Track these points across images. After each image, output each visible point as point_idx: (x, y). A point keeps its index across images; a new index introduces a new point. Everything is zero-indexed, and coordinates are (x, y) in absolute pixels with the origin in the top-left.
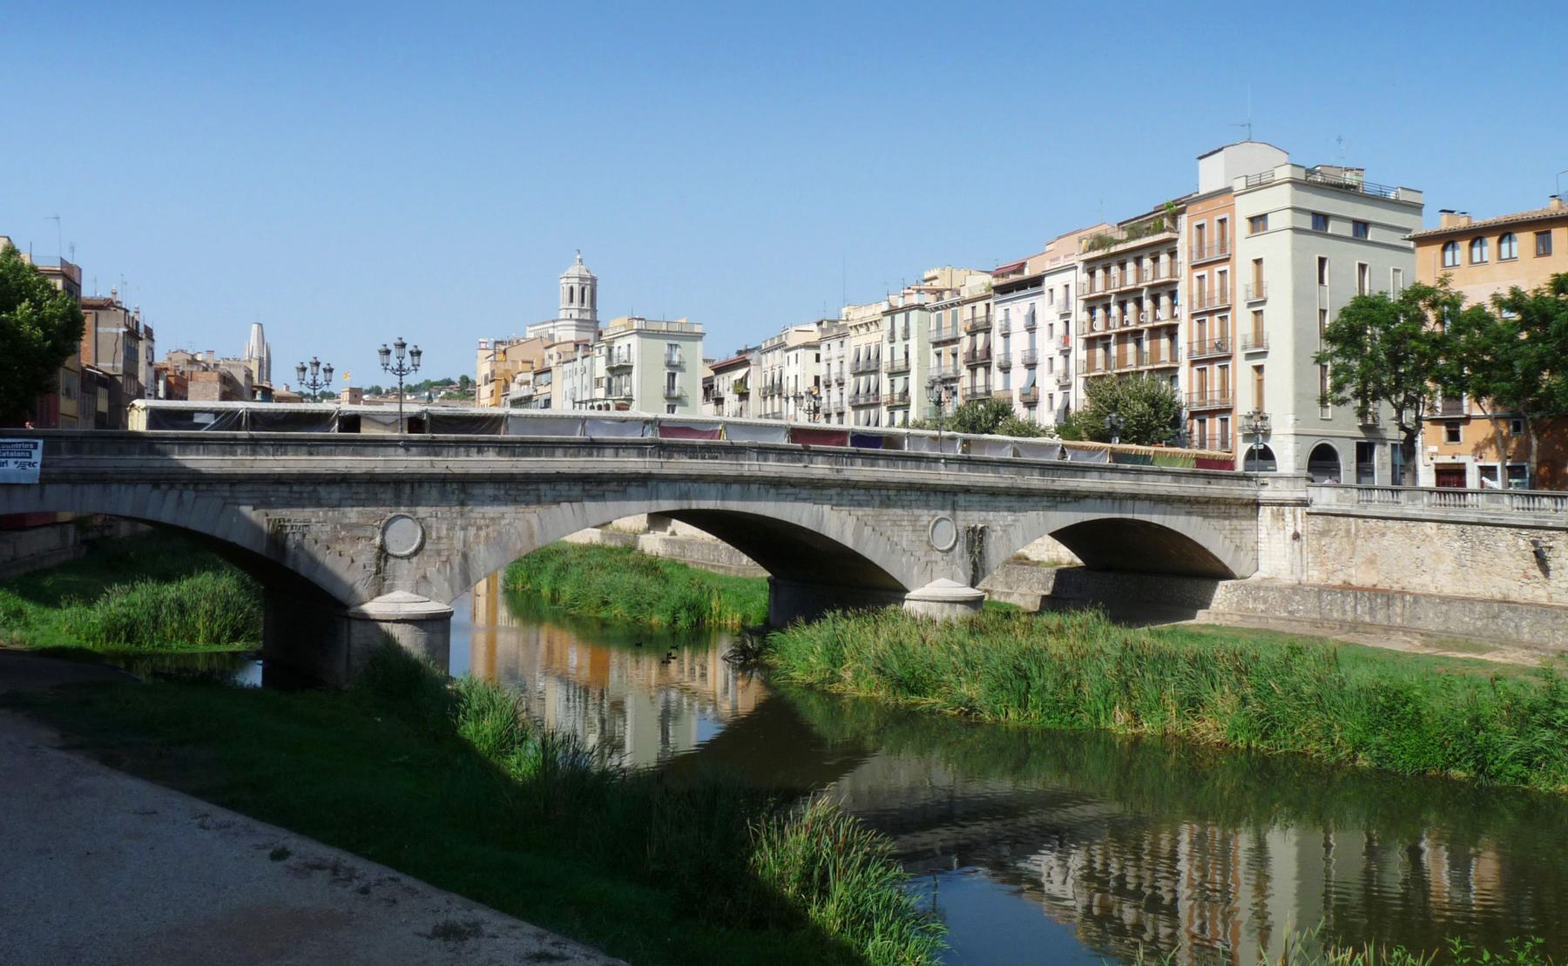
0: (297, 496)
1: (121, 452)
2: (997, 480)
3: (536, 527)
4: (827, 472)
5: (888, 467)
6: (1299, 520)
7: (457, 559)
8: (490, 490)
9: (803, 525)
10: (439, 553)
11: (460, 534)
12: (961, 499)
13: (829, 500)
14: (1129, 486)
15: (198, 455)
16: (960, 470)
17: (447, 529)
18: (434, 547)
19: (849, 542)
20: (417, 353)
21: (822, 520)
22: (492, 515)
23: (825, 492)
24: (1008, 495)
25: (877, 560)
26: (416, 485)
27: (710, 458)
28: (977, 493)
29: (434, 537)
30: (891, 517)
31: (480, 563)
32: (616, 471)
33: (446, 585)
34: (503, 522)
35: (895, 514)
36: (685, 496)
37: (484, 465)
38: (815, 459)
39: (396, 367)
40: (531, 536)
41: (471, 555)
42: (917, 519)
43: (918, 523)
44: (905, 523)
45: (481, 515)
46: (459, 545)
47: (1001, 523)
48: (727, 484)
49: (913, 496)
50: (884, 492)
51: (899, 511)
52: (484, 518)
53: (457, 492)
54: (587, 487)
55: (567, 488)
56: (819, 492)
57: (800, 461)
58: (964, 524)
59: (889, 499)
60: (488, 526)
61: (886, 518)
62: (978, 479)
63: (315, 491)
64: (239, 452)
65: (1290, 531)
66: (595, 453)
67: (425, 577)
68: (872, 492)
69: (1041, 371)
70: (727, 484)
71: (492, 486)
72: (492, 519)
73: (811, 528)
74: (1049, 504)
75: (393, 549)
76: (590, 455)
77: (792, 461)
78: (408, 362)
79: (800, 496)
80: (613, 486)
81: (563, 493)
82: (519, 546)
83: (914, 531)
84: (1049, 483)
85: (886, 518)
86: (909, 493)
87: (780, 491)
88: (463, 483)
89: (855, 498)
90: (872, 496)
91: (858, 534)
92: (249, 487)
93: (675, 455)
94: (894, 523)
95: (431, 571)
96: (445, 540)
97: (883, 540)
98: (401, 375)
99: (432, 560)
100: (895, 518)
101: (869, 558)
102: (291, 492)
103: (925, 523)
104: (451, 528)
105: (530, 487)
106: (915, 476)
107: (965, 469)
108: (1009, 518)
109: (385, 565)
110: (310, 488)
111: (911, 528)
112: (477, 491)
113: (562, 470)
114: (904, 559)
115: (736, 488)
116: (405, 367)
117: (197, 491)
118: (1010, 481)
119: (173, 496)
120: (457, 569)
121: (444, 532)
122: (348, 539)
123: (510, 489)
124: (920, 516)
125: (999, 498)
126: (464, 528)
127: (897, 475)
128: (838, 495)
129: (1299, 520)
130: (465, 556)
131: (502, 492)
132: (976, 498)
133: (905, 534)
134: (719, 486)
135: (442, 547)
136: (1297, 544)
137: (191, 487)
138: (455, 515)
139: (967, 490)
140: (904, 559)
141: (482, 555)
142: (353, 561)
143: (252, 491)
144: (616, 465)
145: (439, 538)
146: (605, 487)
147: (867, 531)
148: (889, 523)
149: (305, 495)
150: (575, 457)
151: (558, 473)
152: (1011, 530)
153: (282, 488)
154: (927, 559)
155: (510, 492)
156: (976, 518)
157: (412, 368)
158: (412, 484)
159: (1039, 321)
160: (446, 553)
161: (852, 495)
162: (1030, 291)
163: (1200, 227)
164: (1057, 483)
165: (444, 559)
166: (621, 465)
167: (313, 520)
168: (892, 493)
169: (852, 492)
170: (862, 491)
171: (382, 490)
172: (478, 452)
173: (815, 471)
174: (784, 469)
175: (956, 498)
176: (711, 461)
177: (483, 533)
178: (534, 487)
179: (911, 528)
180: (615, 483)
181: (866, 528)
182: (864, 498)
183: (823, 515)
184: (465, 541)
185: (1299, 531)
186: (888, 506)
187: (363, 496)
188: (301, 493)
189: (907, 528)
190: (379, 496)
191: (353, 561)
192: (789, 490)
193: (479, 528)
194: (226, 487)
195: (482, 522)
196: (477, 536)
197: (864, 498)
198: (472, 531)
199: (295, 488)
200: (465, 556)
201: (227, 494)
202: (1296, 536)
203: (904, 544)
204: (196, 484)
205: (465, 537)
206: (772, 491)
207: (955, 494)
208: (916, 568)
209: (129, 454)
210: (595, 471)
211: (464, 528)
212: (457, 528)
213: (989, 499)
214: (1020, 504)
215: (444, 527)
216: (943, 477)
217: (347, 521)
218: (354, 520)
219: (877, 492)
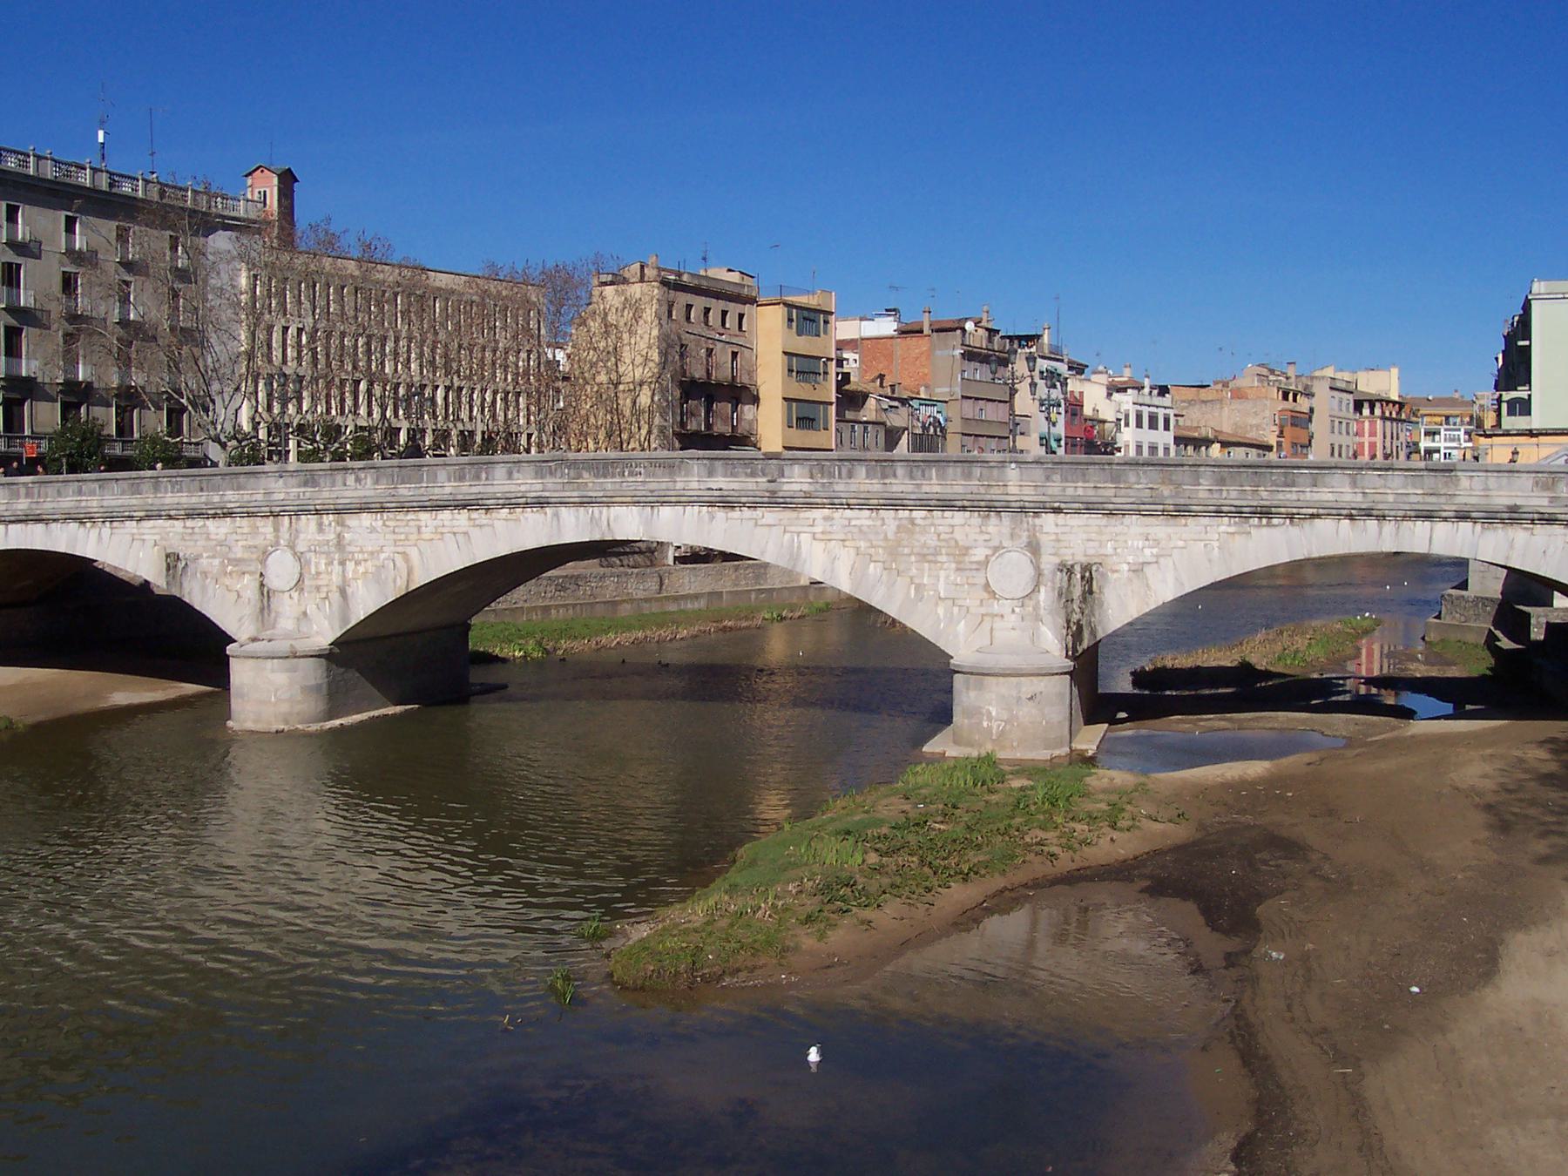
0: (190, 531)
7: (335, 596)
10: (318, 588)
11: (337, 568)
14: (1420, 499)
17: (326, 564)
18: (314, 583)
22: (370, 549)
24: (1139, 513)
27: (631, 474)
29: (313, 571)
30: (915, 551)
31: (359, 601)
33: (326, 623)
34: (383, 556)
40: (410, 573)
41: (349, 591)
43: (967, 559)
44: (943, 558)
45: (358, 549)
47: (1130, 559)
52: (361, 552)
53: (333, 524)
56: (793, 514)
58: (1057, 560)
59: (913, 524)
60: (366, 560)
61: (906, 551)
67: (305, 614)
72: (372, 553)
74: (1231, 529)
75: (273, 582)
79: (764, 521)
81: (446, 523)
83: (958, 569)
85: (906, 551)
86: (947, 514)
89: (853, 523)
90: (883, 519)
92: (151, 523)
94: (923, 557)
97: (901, 582)
99: (313, 595)
100: (925, 551)
102: (185, 527)
103: (982, 558)
104: (330, 563)
108: (1147, 552)
111: (953, 566)
114: (941, 611)
117: (112, 528)
119: (94, 533)
120: (335, 607)
122: (234, 575)
124: (968, 548)
126: (342, 563)
128: (826, 519)
130: (343, 592)
131: (380, 523)
133: (942, 573)
135: (320, 583)
137: (108, 524)
138: (333, 549)
141: (360, 593)
142: (239, 596)
143: (154, 527)
145: (318, 573)
148: (913, 558)
149: (196, 530)
152: (1148, 570)
154: (983, 610)
155: (387, 523)
160: (325, 589)
161: (850, 520)
165: (324, 595)
171: (262, 524)
175: (1037, 521)
176: (631, 479)
177: (361, 569)
179: (953, 566)
181: (872, 565)
182: (870, 522)
183: (799, 547)
184: (344, 576)
187: (246, 530)
188: (193, 528)
189: (946, 566)
190: (260, 530)
191: (239, 596)
193: (358, 563)
195: (361, 556)
196: (355, 571)
197: (870, 522)
199: (189, 523)
200: (343, 592)
201: (135, 531)
211: (342, 563)
212: (336, 562)
213: (1104, 521)
214: (1170, 530)
215: (323, 562)
217: (232, 556)
218: (239, 555)
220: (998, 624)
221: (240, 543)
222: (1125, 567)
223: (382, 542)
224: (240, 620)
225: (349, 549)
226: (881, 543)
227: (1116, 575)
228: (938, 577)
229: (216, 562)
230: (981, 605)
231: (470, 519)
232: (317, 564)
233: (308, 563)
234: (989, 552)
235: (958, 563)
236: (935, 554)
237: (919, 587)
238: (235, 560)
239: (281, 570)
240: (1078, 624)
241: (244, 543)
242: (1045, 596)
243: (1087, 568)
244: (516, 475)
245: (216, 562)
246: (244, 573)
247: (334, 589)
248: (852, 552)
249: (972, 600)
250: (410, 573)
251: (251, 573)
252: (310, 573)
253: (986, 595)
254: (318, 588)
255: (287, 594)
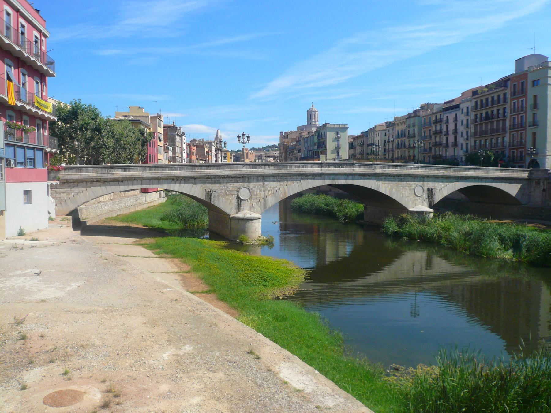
1: (163, 170)
2: (439, 173)
3: (286, 190)
4: (381, 171)
5: (401, 169)
6: (545, 185)
7: (262, 201)
8: (272, 179)
9: (373, 188)
10: (257, 199)
12: (426, 179)
13: (381, 180)
15: (185, 170)
16: (426, 170)
19: (388, 194)
20: (248, 137)
21: (379, 187)
23: (380, 178)
24: (442, 178)
25: (397, 200)
26: (249, 178)
27: (342, 167)
28: (431, 177)
32: (311, 172)
34: (276, 189)
35: (403, 185)
36: (334, 179)
37: (271, 171)
38: (376, 167)
39: (243, 141)
40: (285, 193)
41: (267, 199)
42: (411, 186)
43: (411, 188)
44: (407, 187)
46: (263, 196)
48: (347, 176)
49: (410, 178)
50: (400, 177)
51: (404, 183)
52: (270, 188)
54: (302, 177)
55: (296, 178)
57: (372, 168)
60: (271, 190)
62: (431, 173)
63: (219, 180)
64: (197, 169)
65: (542, 188)
66: (305, 167)
68: (396, 177)
69: (459, 136)
70: (347, 176)
71: (273, 177)
72: (273, 188)
73: (375, 189)
76: (303, 167)
77: (369, 168)
78: (246, 140)
80: (311, 177)
82: (281, 196)
83: (410, 190)
84: (456, 174)
85: (400, 186)
86: (408, 178)
87: (365, 178)
88: (264, 177)
91: (391, 190)
92: (199, 180)
93: (331, 167)
94: (403, 188)
95: (255, 204)
96: (258, 195)
98: (244, 144)
99: (255, 201)
100: (404, 186)
101: (395, 199)
102: (212, 181)
103: (414, 187)
105: (284, 178)
106: (410, 172)
107: (427, 169)
108: (443, 185)
109: (241, 203)
110: (218, 179)
112: (268, 179)
113: (294, 172)
115: (350, 177)
116: (245, 141)
118: (443, 173)
120: (262, 204)
121: (258, 192)
123: (278, 179)
124: (411, 185)
125: (439, 179)
126: (264, 191)
127: (404, 172)
128: (385, 178)
129: (545, 185)
131: (276, 179)
132: (431, 179)
133: (407, 191)
134: (345, 176)
135: (258, 197)
136: (544, 193)
138: (261, 187)
139: (428, 176)
140: (406, 199)
142: (231, 202)
144: (312, 170)
145: (257, 194)
146: (308, 177)
147: (394, 190)
148: (401, 187)
149: (216, 182)
150: (298, 168)
151: (293, 173)
152: (443, 189)
153: (209, 180)
156: (431, 185)
157: (247, 142)
158: (248, 177)
159: (458, 119)
160: (259, 199)
162: (455, 109)
163: (515, 85)
164: (459, 174)
166: (313, 170)
167: (219, 189)
168: (402, 178)
169: (389, 177)
170: (392, 177)
171: (239, 180)
172: (268, 167)
173: (376, 171)
174: (366, 171)
175: (424, 179)
177: (270, 193)
178: (286, 178)
180: (311, 176)
185: (545, 188)
186: (401, 181)
188: (215, 181)
191: (231, 202)
192: (368, 177)
193: (269, 191)
194: (193, 180)
196: (268, 193)
198: (267, 192)
199: (213, 180)
202: (544, 190)
203: (407, 194)
204: (184, 179)
205: (265, 193)
206: (362, 177)
207: (424, 178)
208: (410, 202)
209: (166, 171)
210: (305, 172)
211: (264, 191)
212: (262, 191)
213: (435, 179)
216: (420, 172)
217: (229, 189)
219: (397, 177)
220: (417, 202)
221: (231, 186)
222: (439, 189)
223: (276, 185)
224: (231, 208)
225: (268, 187)
226: (395, 184)
227: (437, 191)
228: (406, 192)
229: (223, 192)
230: (414, 197)
231: (301, 178)
232: (256, 191)
233: (254, 191)
234: (415, 186)
235: (410, 188)
236: (405, 187)
237: (403, 194)
238: (230, 190)
239: (244, 194)
240: (431, 201)
241: (233, 185)
242: (425, 195)
243: (432, 189)
244: (313, 167)
245: (223, 192)
246: (232, 195)
247: (262, 199)
248: (390, 186)
249: (412, 196)
250: (285, 193)
251: (235, 194)
252: (254, 194)
253: (415, 195)
254: (257, 199)
255: (247, 201)
